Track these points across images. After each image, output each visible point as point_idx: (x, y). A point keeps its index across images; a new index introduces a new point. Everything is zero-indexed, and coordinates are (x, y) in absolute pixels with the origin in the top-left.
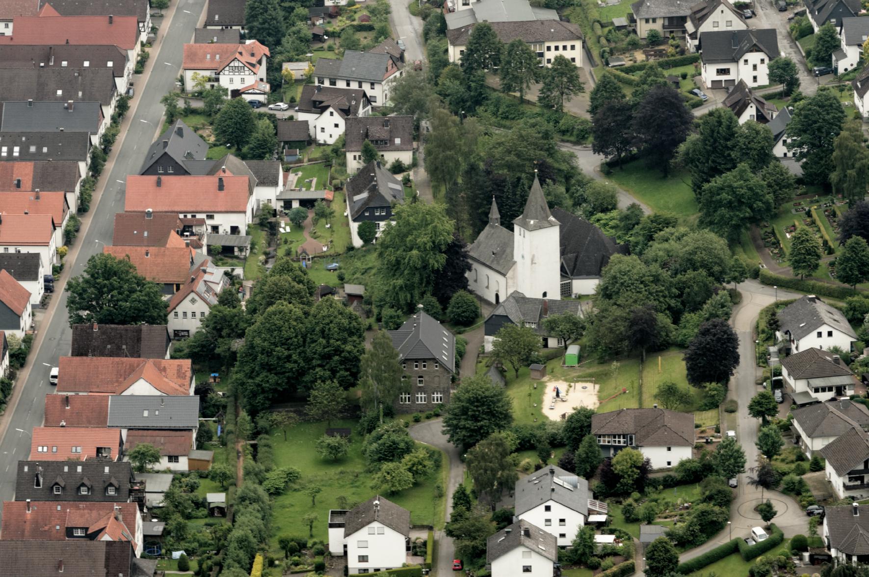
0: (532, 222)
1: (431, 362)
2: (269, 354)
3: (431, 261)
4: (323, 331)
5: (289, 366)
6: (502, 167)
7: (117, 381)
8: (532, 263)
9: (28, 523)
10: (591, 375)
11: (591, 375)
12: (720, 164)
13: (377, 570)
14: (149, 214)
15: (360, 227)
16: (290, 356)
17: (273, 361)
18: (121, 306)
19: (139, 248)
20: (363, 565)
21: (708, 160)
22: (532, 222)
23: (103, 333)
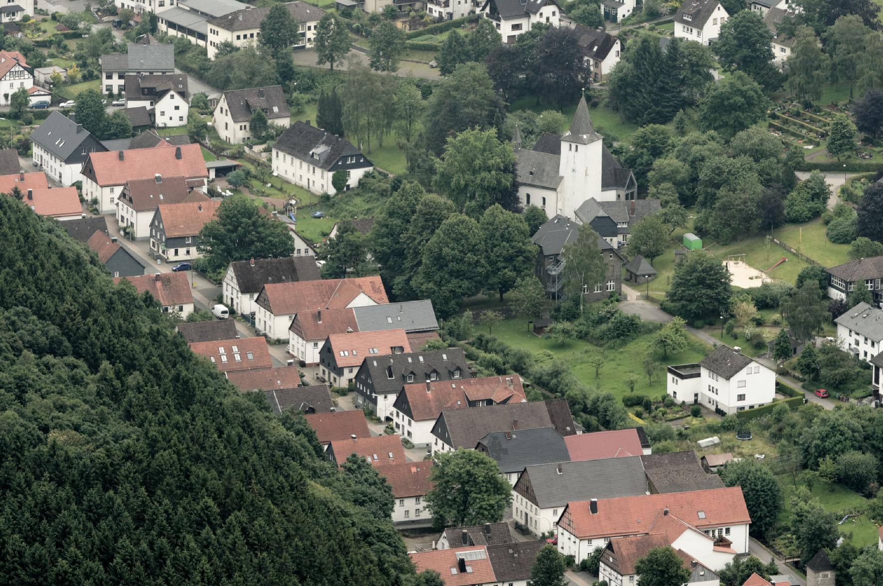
0: (585, 137)
1: (607, 253)
2: (460, 261)
3: (503, 180)
4: (502, 236)
5: (480, 269)
6: (466, 106)
7: (323, 301)
8: (586, 175)
9: (432, 402)
10: (730, 253)
11: (730, 253)
12: (667, 83)
13: (752, 407)
14: (158, 179)
15: (334, 177)
16: (478, 261)
17: (464, 268)
18: (270, 241)
19: (191, 204)
20: (741, 404)
21: (655, 81)
22: (585, 137)
23: (261, 267)
